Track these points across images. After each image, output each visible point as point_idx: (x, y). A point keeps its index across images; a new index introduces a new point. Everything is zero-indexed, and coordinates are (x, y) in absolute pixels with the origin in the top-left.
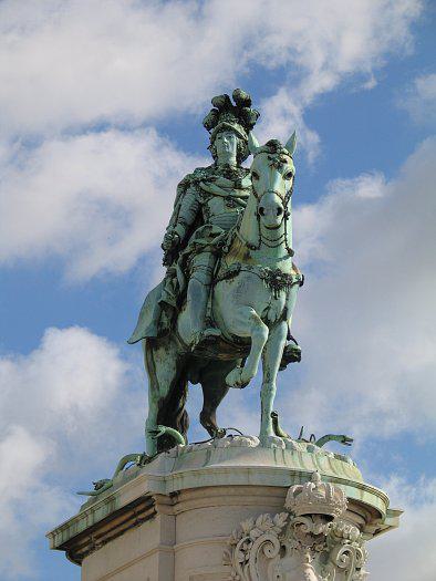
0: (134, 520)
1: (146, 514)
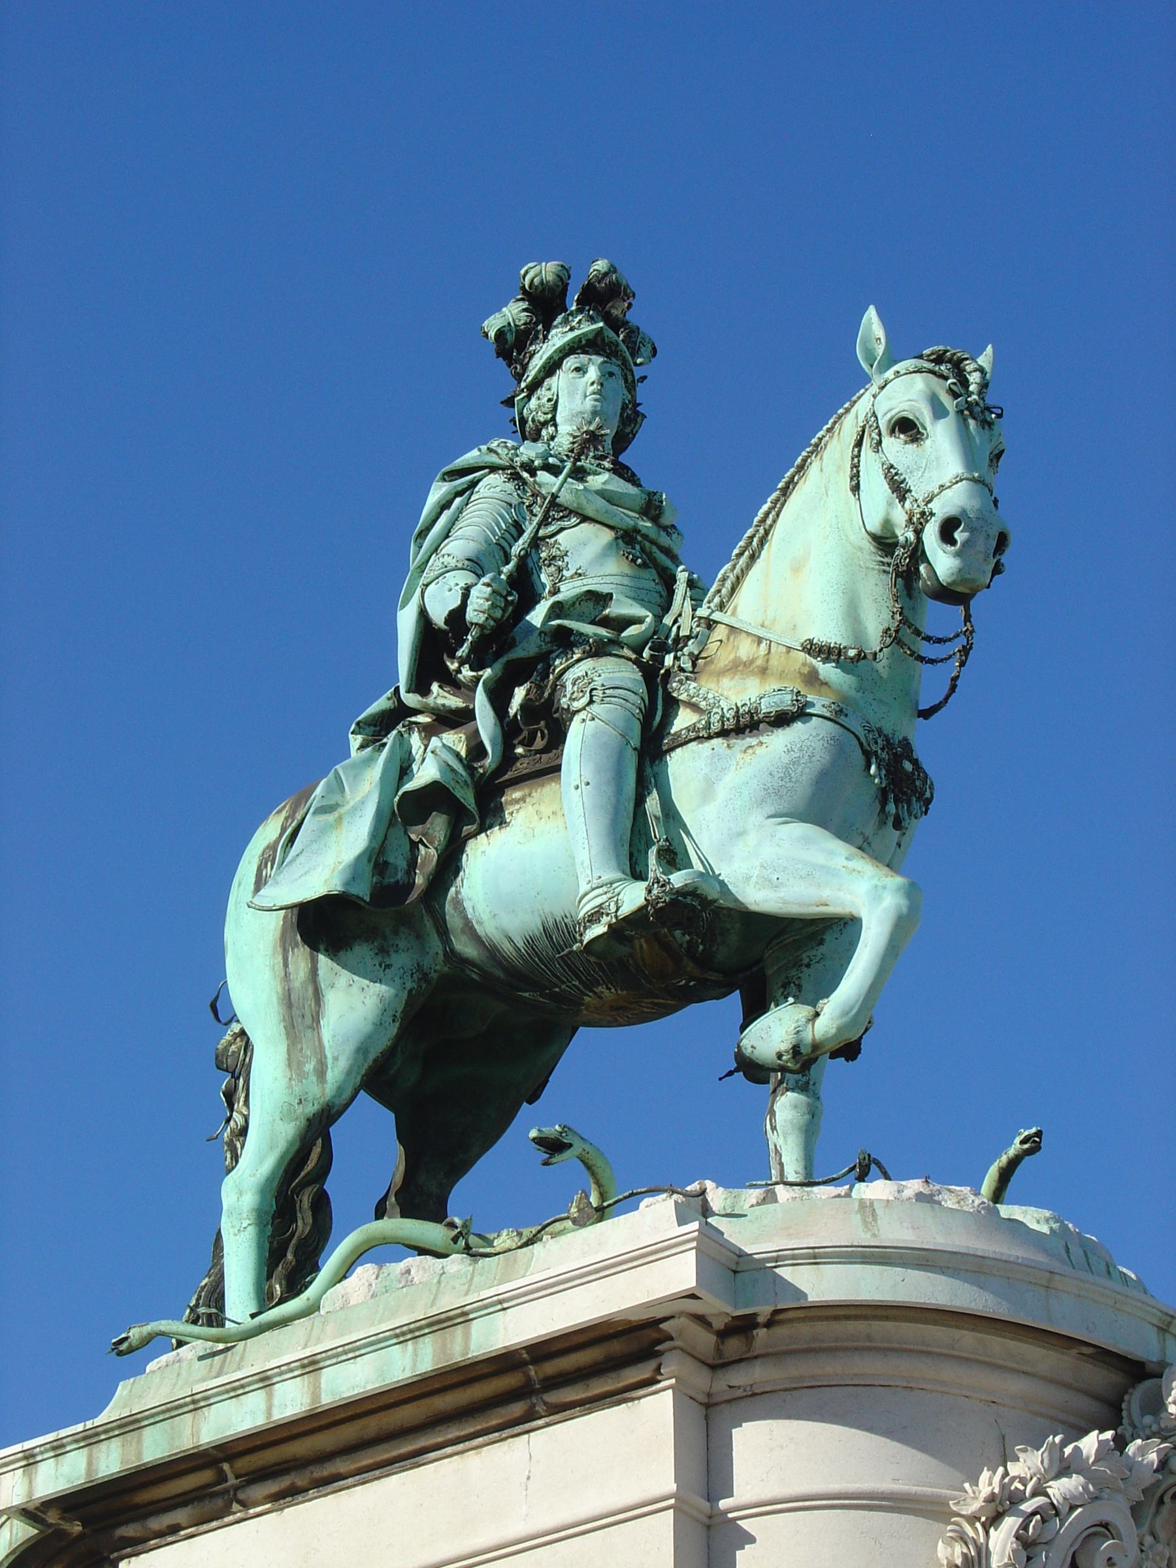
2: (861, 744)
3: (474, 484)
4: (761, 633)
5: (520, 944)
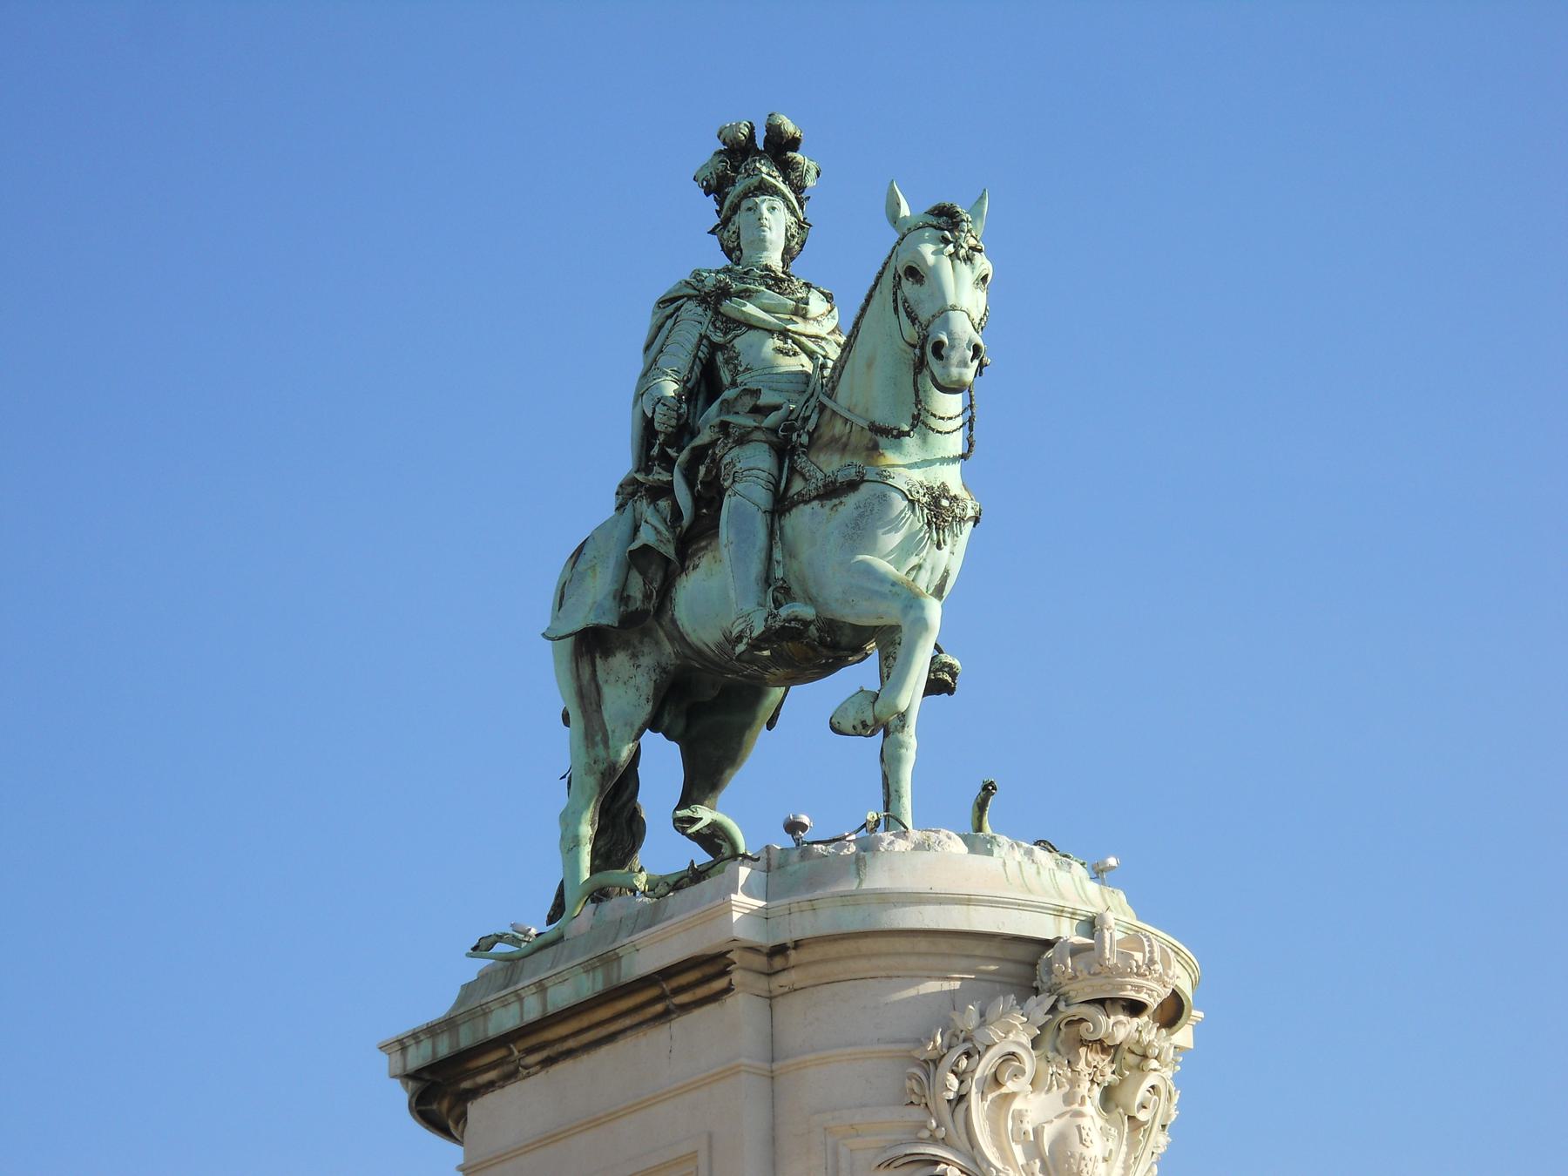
0: (659, 1007)
1: (701, 992)
3: (678, 309)
4: (847, 415)
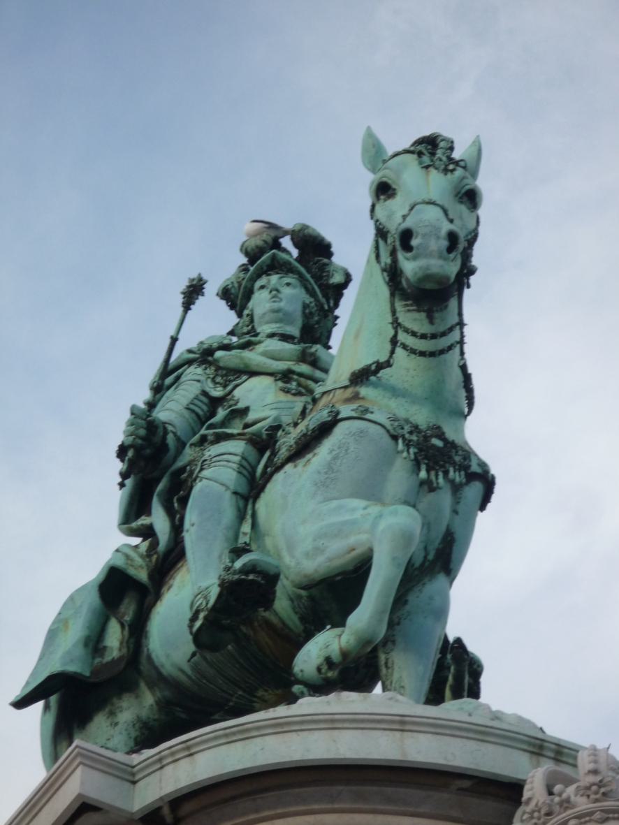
2: (388, 431)
5: (189, 671)
